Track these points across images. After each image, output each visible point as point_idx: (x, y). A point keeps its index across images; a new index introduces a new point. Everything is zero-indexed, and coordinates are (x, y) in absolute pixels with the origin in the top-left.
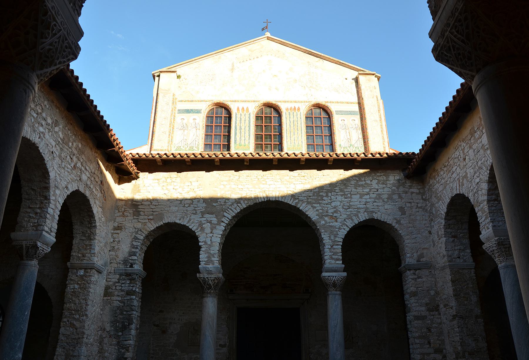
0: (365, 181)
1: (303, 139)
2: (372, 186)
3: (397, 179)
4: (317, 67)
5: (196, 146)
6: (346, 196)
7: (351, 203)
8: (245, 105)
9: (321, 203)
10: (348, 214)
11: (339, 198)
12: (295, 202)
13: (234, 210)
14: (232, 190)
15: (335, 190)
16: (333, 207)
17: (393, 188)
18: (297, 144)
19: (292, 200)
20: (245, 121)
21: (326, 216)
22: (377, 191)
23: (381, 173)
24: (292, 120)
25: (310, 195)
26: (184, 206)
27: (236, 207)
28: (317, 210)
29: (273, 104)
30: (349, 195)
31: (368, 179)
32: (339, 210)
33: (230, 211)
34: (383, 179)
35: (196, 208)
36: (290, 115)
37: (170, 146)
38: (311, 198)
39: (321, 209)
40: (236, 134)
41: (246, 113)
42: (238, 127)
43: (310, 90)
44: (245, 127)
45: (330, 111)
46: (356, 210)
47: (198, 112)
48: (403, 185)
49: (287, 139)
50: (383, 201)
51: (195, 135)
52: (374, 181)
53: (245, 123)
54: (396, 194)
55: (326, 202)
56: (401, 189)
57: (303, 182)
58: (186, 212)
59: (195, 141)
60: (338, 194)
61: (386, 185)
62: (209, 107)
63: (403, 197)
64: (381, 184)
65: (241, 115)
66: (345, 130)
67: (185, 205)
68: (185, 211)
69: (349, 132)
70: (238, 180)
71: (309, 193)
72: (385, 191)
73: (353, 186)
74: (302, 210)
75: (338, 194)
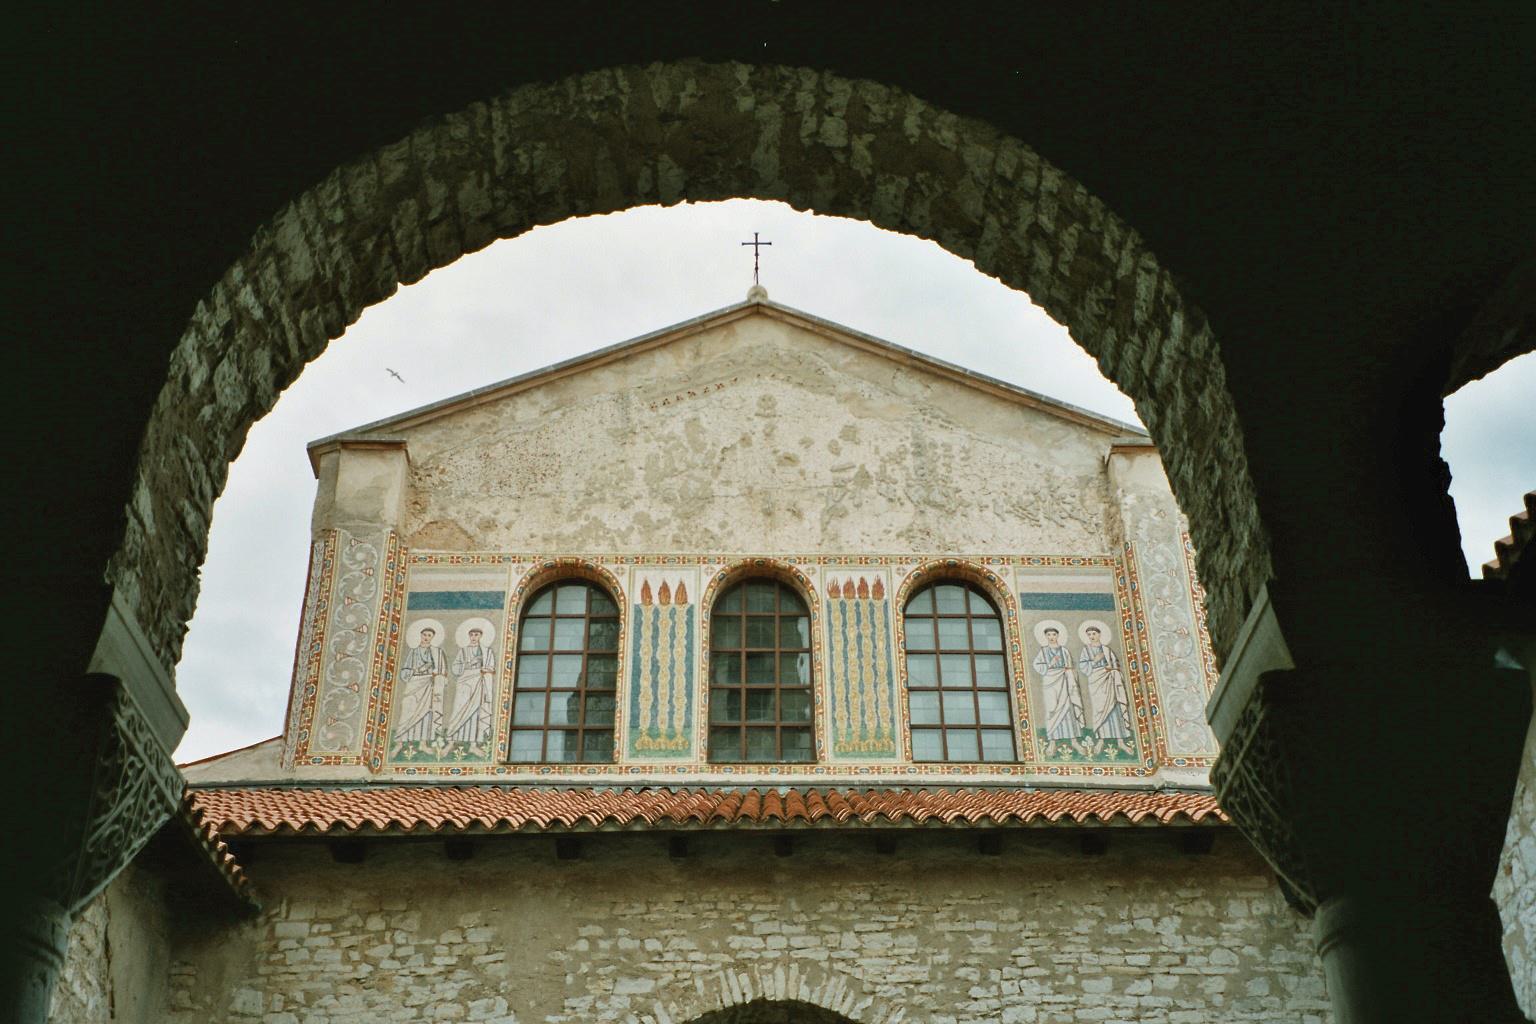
0: (1131, 920)
1: (896, 710)
2: (1161, 943)
3: (1259, 913)
4: (950, 423)
5: (481, 739)
6: (1057, 983)
7: (1080, 1014)
9: (963, 1011)
11: (1033, 990)
14: (623, 959)
15: (1015, 956)
17: (1248, 950)
18: (871, 725)
19: (849, 1000)
20: (673, 636)
22: (1183, 961)
23: (1193, 887)
24: (852, 635)
25: (918, 978)
29: (779, 568)
30: (1071, 980)
31: (1142, 913)
34: (1201, 913)
36: (843, 612)
38: (923, 988)
40: (636, 690)
44: (673, 661)
47: (491, 601)
48: (1287, 938)
50: (1210, 1005)
51: (477, 698)
52: (1166, 920)
53: (672, 646)
54: (1254, 975)
55: (981, 1006)
56: (1281, 956)
59: (475, 718)
61: (1217, 937)
62: (534, 582)
63: (1290, 988)
64: (1197, 934)
65: (656, 612)
66: (1060, 672)
69: (1078, 682)
70: (646, 917)
71: (913, 969)
72: (1217, 963)
73: (1086, 940)
75: (1028, 972)
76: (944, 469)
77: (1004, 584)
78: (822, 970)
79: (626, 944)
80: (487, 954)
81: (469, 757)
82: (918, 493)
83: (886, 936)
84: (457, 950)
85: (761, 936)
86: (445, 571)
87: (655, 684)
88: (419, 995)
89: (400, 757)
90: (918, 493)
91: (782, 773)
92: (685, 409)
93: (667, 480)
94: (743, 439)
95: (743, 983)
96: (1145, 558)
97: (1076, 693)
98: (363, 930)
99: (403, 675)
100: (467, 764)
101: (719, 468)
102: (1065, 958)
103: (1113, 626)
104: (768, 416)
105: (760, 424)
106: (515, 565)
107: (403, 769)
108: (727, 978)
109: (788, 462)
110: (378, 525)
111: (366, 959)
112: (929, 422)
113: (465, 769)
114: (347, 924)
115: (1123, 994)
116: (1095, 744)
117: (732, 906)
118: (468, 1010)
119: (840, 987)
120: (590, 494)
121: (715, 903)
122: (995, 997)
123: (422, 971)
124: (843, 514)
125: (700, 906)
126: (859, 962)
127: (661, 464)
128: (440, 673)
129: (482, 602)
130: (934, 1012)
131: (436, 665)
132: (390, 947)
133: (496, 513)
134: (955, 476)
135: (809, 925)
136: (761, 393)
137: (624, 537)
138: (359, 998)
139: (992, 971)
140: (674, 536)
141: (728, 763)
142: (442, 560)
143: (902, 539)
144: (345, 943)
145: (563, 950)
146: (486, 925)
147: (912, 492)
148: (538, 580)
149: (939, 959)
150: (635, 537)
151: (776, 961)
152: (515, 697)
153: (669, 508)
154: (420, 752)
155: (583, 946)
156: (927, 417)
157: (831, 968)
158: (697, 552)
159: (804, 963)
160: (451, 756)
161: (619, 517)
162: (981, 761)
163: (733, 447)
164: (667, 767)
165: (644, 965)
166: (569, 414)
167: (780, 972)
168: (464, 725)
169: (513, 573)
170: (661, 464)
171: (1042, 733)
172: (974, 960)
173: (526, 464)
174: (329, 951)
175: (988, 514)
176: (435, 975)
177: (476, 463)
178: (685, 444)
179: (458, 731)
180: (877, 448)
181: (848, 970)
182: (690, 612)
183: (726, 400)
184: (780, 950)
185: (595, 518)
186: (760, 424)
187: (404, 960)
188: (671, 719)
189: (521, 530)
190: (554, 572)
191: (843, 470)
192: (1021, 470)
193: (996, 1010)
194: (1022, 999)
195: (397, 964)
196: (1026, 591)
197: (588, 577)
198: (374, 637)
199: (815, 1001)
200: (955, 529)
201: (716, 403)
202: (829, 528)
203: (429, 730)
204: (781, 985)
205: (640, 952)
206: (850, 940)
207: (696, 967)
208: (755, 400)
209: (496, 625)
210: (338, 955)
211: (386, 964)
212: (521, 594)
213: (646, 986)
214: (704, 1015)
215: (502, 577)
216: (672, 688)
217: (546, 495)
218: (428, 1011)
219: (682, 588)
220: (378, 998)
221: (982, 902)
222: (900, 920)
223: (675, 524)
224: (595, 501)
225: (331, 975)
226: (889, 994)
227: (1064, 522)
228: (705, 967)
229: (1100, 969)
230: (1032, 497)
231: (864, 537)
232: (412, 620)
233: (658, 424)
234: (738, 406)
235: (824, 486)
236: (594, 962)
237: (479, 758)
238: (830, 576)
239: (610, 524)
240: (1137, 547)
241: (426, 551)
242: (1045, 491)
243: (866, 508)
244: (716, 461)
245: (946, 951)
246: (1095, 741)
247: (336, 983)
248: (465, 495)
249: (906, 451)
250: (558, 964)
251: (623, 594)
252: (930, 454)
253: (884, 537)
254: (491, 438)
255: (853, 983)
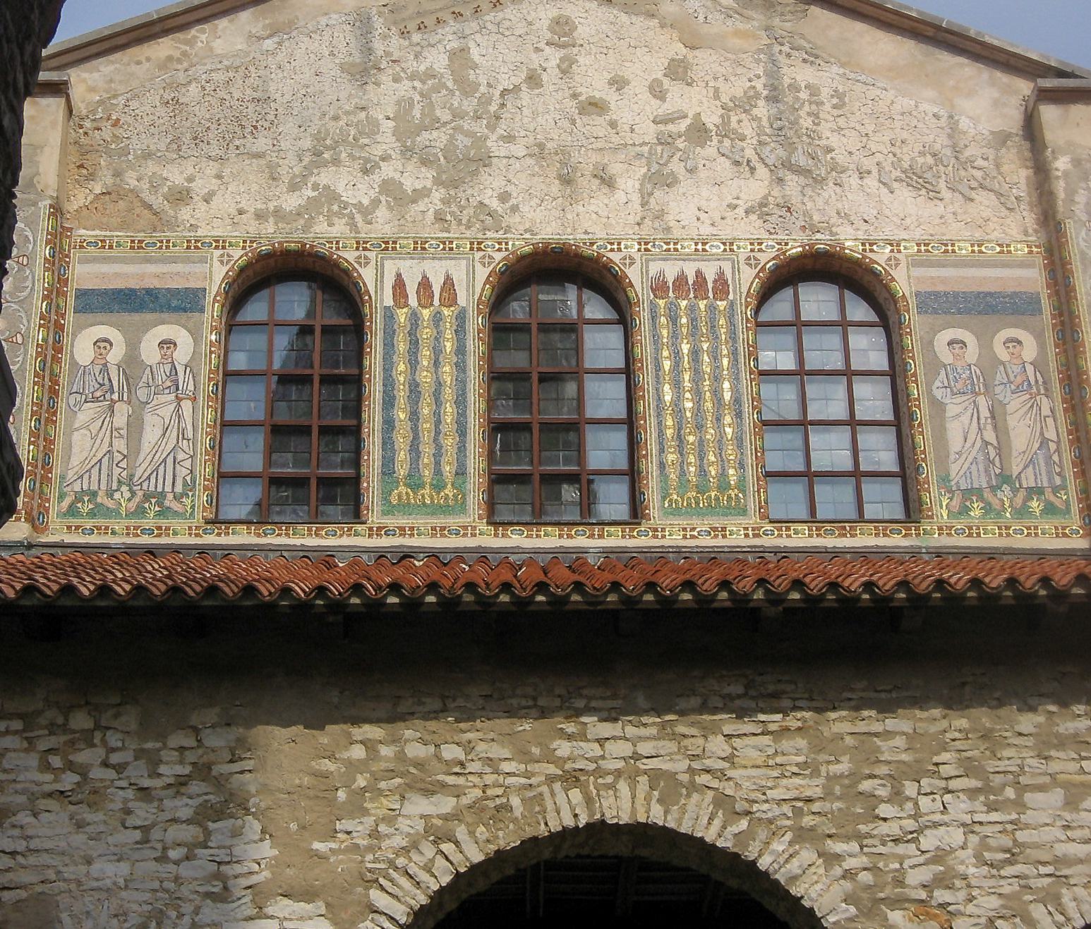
5: (179, 489)
6: (992, 797)
7: (1021, 836)
8: (437, 272)
9: (869, 835)
10: (1007, 890)
11: (960, 808)
12: (735, 829)
13: (423, 876)
14: (413, 770)
15: (937, 764)
16: (928, 856)
19: (717, 823)
21: (897, 902)
25: (808, 793)
26: (163, 859)
27: (432, 860)
28: (848, 875)
29: (582, 257)
30: (1010, 793)
32: (961, 868)
33: (404, 882)
35: (223, 868)
36: (674, 319)
37: (37, 491)
38: (816, 807)
39: (865, 869)
40: (389, 424)
41: (446, 312)
42: (402, 395)
43: (781, 180)
45: (887, 295)
46: (1049, 869)
49: (662, 451)
53: (436, 364)
55: (892, 829)
57: (773, 727)
58: (172, 886)
59: (170, 460)
60: (953, 784)
62: (244, 276)
67: (165, 849)
68: (165, 884)
69: (992, 412)
71: (801, 782)
73: (1029, 742)
74: (771, 870)
75: (953, 784)
76: (810, 120)
77: (893, 279)
78: (682, 785)
79: (416, 750)
80: (231, 761)
81: (164, 512)
82: (774, 153)
83: (766, 740)
84: (191, 757)
85: (598, 741)
86: (124, 261)
87: (414, 416)
88: (143, 813)
89: (72, 511)
90: (774, 153)
91: (592, 536)
92: (448, 36)
93: (426, 135)
94: (530, 78)
95: (574, 802)
96: (1082, 244)
97: (989, 427)
98: (65, 728)
99: (72, 402)
100: (164, 523)
101: (498, 118)
102: (1002, 766)
103: (1039, 336)
104: (564, 46)
105: (553, 57)
106: (217, 253)
107: (77, 528)
108: (553, 794)
109: (598, 110)
110: (32, 197)
111: (70, 766)
112: (789, 55)
113: (159, 528)
114: (43, 721)
115: (1077, 810)
116: (1015, 496)
117: (557, 702)
118: (208, 833)
119: (705, 804)
120: (318, 154)
121: (535, 699)
122: (910, 816)
123: (146, 783)
124: (669, 182)
125: (514, 702)
126: (730, 773)
127: (417, 112)
128: (121, 399)
129: (174, 303)
130: (830, 836)
131: (116, 389)
132: (100, 752)
133: (190, 179)
134: (825, 129)
135: (663, 726)
136: (553, 13)
137: (367, 212)
138: (64, 817)
139: (907, 783)
140: (436, 212)
141: (518, 524)
142: (119, 245)
143: (753, 217)
144: (43, 745)
145: (331, 757)
146: (229, 725)
147: (766, 151)
148: (250, 272)
149: (835, 769)
150: (382, 213)
151: (618, 773)
152: (221, 433)
153: (428, 174)
154: (98, 505)
155: (358, 752)
156: (786, 49)
157: (692, 782)
158: (468, 234)
159: (655, 777)
160: (140, 512)
161: (359, 186)
162: (861, 518)
163: (517, 88)
164: (433, 529)
165: (441, 777)
166: (287, 44)
167: (623, 787)
168: (157, 469)
169: (216, 264)
170: (417, 112)
171: (944, 479)
172: (883, 770)
173: (228, 113)
174: (22, 755)
175: (871, 182)
176: (164, 788)
177: (161, 111)
178: (450, 84)
179: (149, 478)
180: (716, 90)
181: (715, 784)
182: (461, 317)
183: (507, 23)
184: (623, 758)
185: (327, 187)
186: (553, 57)
187: (120, 768)
188: (438, 463)
189: (224, 203)
190: (272, 261)
191: (672, 121)
192: (915, 122)
193: (911, 833)
194: (946, 818)
195: (111, 774)
196: (924, 288)
197: (318, 269)
198: (32, 351)
199: (671, 824)
200: (827, 203)
201: (493, 28)
202: (652, 200)
203: (110, 476)
204: (626, 804)
205: (434, 762)
206: (717, 745)
207: (511, 780)
208: (546, 23)
209: (196, 335)
210: (33, 760)
211: (97, 773)
212: (227, 293)
213: (446, 804)
214: (522, 842)
215: (198, 268)
216: (438, 423)
217: (258, 156)
218: (156, 834)
219: (449, 284)
220: (89, 817)
221: (894, 695)
222: (783, 719)
223: (438, 195)
224: (325, 164)
225: (27, 785)
226: (770, 815)
227: (973, 194)
228: (523, 781)
229: (1047, 779)
230: (930, 160)
231: (702, 216)
232: (79, 328)
233: (412, 57)
234: (521, 32)
235: (644, 144)
236: (373, 774)
237: (176, 514)
238: (654, 268)
239: (348, 196)
240: (1070, 227)
241: (97, 232)
242: (948, 152)
243: (703, 174)
244: (493, 108)
245: (845, 758)
246: (1015, 491)
247: (33, 798)
248: (148, 155)
249: (757, 96)
250: (326, 776)
251: (367, 292)
252: (789, 99)
253: (729, 214)
254: (181, 78)
255: (722, 801)
